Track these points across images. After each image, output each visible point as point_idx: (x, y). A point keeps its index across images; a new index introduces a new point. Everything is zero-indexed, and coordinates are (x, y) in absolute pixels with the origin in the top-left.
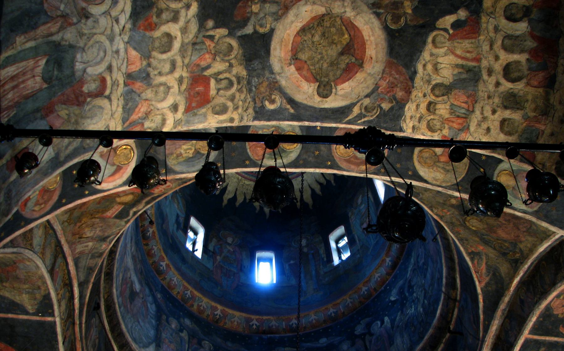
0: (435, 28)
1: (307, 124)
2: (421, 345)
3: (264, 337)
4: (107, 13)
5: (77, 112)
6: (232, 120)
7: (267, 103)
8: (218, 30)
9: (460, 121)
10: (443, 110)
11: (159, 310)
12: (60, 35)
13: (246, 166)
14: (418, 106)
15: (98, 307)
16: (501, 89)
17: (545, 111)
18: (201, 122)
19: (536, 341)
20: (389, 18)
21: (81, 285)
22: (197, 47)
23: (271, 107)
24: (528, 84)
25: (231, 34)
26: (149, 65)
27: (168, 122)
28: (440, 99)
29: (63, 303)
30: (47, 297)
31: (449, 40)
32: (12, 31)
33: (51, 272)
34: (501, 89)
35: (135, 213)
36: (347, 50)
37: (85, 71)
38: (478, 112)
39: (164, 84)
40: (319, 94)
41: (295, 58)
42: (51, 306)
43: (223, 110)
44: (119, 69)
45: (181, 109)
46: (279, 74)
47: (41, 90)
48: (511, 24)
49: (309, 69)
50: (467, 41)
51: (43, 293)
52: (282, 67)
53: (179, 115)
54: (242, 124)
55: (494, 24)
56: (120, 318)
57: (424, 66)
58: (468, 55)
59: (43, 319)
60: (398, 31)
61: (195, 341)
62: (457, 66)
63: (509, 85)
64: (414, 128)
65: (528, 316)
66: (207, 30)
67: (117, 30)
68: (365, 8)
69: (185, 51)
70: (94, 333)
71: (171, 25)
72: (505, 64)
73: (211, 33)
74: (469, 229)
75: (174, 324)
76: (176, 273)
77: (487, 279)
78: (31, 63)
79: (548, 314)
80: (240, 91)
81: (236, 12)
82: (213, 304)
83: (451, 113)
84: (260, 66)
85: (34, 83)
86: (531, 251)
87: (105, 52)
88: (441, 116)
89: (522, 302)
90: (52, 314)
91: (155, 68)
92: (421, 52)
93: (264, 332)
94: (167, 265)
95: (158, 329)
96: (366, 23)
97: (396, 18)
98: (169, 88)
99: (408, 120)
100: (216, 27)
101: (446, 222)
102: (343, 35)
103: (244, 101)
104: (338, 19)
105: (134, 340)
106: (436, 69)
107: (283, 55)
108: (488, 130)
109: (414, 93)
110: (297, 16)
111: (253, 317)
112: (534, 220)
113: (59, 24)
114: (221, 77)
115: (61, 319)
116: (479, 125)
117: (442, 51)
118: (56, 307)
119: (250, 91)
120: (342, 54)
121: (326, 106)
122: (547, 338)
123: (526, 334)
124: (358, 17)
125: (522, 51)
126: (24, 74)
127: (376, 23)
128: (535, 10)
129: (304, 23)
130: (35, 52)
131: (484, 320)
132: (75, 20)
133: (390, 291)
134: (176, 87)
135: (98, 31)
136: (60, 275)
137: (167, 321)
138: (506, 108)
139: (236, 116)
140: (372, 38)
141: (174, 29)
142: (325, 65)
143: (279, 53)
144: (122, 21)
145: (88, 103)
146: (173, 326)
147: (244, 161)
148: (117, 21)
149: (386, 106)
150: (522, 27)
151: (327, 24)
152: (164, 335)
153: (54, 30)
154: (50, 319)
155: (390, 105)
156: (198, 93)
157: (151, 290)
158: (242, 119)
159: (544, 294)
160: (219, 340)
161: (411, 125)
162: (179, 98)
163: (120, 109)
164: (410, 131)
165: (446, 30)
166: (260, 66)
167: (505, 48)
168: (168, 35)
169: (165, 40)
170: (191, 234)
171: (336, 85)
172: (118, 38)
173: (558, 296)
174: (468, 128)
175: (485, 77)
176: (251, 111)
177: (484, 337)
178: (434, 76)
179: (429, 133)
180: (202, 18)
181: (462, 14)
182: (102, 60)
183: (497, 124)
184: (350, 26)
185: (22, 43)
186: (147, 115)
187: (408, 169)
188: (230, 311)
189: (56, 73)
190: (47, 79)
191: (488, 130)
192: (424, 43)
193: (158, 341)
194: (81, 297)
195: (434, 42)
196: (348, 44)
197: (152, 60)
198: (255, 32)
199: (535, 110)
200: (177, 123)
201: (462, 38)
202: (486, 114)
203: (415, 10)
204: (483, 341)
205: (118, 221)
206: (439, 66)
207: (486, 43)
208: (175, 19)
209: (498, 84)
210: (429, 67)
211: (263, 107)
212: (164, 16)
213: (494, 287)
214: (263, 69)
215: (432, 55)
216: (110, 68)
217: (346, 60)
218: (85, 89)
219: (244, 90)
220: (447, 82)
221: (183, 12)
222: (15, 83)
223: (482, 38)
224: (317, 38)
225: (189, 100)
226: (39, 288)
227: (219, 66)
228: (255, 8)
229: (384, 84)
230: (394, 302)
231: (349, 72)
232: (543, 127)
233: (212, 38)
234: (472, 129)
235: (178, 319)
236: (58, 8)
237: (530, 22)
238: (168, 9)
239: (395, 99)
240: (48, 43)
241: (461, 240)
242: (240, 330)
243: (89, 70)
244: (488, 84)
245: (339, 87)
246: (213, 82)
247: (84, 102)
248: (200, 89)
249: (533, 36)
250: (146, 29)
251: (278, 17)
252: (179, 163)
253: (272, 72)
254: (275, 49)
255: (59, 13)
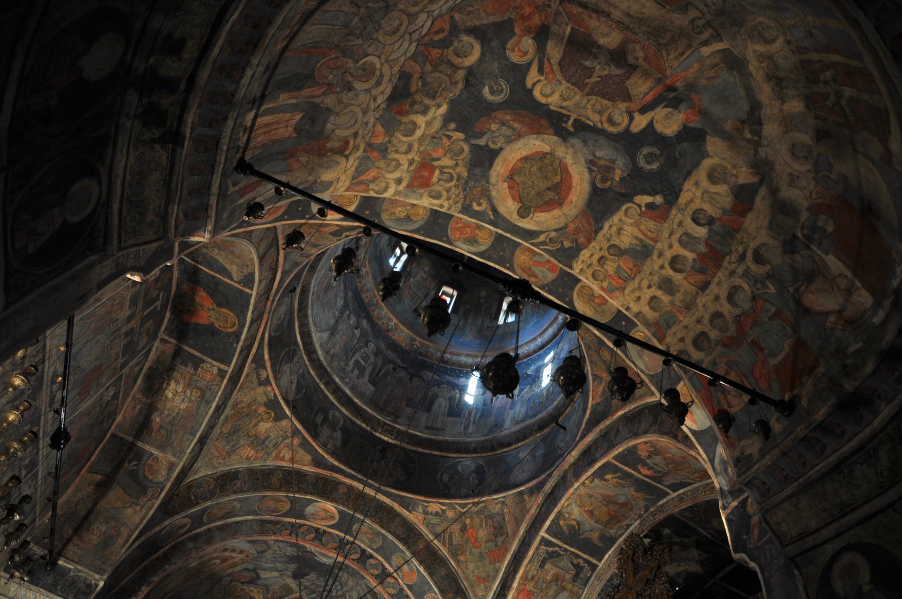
0: (632, 201)
1: (500, 231)
2: (533, 420)
3: (420, 357)
4: (368, 91)
5: (315, 161)
6: (442, 206)
7: (474, 204)
8: (457, 133)
9: (620, 281)
10: (610, 267)
11: (346, 305)
12: (322, 98)
13: (442, 241)
14: (592, 255)
15: (294, 290)
16: (663, 272)
17: (689, 306)
18: (416, 199)
19: (616, 466)
20: (599, 177)
21: (284, 273)
22: (435, 141)
23: (476, 208)
24: (686, 278)
25: (466, 140)
26: (390, 142)
27: (390, 190)
28: (612, 257)
29: (263, 284)
30: (252, 275)
31: (639, 215)
32: (279, 88)
33: (261, 259)
34: (663, 272)
35: (347, 236)
36: (556, 188)
37: (333, 131)
38: (637, 281)
39: (397, 161)
40: (518, 213)
41: (510, 178)
42: (253, 283)
43: (438, 196)
44: (363, 137)
45: (404, 184)
46: (493, 185)
47: (290, 138)
48: (694, 225)
49: (518, 191)
50: (653, 222)
51: (249, 270)
52: (498, 181)
53: (401, 188)
54: (449, 212)
55: (680, 217)
56: (310, 303)
57: (611, 226)
58: (649, 234)
59: (243, 288)
60: (602, 190)
61: (364, 340)
62: (637, 238)
63: (671, 272)
64: (581, 270)
65: (617, 445)
66: (448, 130)
67: (372, 106)
68: (582, 161)
69: (424, 140)
70: (283, 309)
71: (419, 116)
72: (675, 254)
73: (450, 133)
74: (600, 357)
75: (353, 321)
76: (371, 280)
77: (599, 400)
78: (288, 115)
79: (633, 450)
80: (457, 186)
81: (477, 124)
82: (391, 316)
83: (615, 272)
84: (480, 174)
85: (285, 132)
86: (641, 397)
87: (356, 121)
88: (607, 270)
89: (618, 431)
90: (252, 290)
91: (394, 146)
92: (613, 214)
93: (421, 354)
94: (367, 273)
95: (337, 321)
96: (579, 174)
97: (604, 180)
98: (400, 164)
99: (579, 263)
100: (456, 130)
101: (585, 344)
102: (557, 175)
103: (457, 196)
104: (557, 161)
105: (315, 324)
106: (619, 231)
107: (502, 171)
108: (639, 298)
109: (593, 244)
110: (525, 145)
111: (417, 338)
112: (647, 381)
113: (323, 90)
114: (445, 170)
115: (257, 293)
116: (633, 291)
117: (630, 221)
118: (256, 284)
119: (465, 190)
120: (549, 189)
121: (520, 224)
122: (626, 468)
123: (609, 458)
124: (574, 166)
125: (692, 251)
126: (279, 123)
127: (587, 176)
128: (718, 223)
129: (529, 153)
130: (294, 108)
131: (584, 429)
132: (338, 90)
133: (530, 365)
134: (406, 166)
135: (355, 103)
136: (269, 260)
137: (348, 317)
138: (660, 288)
139: (446, 204)
140: (578, 187)
141: (421, 120)
142: (533, 193)
143: (499, 169)
144: (379, 101)
145: (328, 157)
146: (351, 322)
147: (443, 237)
148: (375, 99)
149: (567, 244)
150: (701, 232)
151: (547, 161)
152: (341, 327)
153: (317, 93)
154: (248, 291)
155: (570, 245)
156: (422, 177)
157: (345, 287)
158: (449, 208)
159: (636, 435)
160: (383, 346)
161: (580, 267)
162: (405, 174)
163: (353, 169)
164: (577, 271)
165: (640, 206)
166: (480, 174)
167: (680, 241)
168: (414, 123)
169: (410, 126)
170: (398, 251)
171: (535, 211)
172: (370, 113)
173: (646, 443)
174: (624, 290)
175: (655, 257)
176: (459, 205)
177: (579, 442)
178: (614, 238)
179: (592, 280)
180: (447, 119)
181: (659, 199)
182: (352, 126)
183: (648, 297)
184: (564, 170)
185: (285, 99)
186: (374, 179)
187: (567, 296)
188: (402, 327)
189: (307, 127)
190: (298, 129)
191: (639, 298)
192: (618, 208)
193: (333, 331)
194: (282, 281)
195: (626, 211)
196: (557, 184)
197: (394, 139)
198: (487, 145)
199: (682, 301)
200: (397, 193)
201: (650, 218)
202: (642, 286)
203: (622, 179)
204: (577, 444)
205: (331, 237)
206: (622, 232)
207: (667, 231)
208: (424, 112)
209: (662, 267)
210: (614, 229)
211: (471, 205)
212: (416, 107)
213: (602, 408)
214: (482, 176)
215: (620, 220)
216: (356, 135)
217: (551, 195)
218: (329, 145)
219: (460, 187)
220: (623, 247)
221: (433, 110)
222: (268, 129)
223: (666, 225)
224: (534, 169)
225: (413, 179)
226: (248, 266)
227: (447, 161)
228: (494, 127)
229: (572, 227)
230: (529, 376)
231: (548, 206)
232: (682, 318)
233: (449, 137)
234: (626, 292)
235: (358, 317)
236: (326, 78)
237: (710, 230)
238: (421, 103)
239: (576, 242)
240: (308, 103)
241: (591, 362)
242: (403, 344)
243: (337, 132)
244: (654, 263)
245: (536, 214)
246: (437, 172)
247: (324, 155)
248: (426, 174)
249: (707, 244)
250: (397, 113)
251: (510, 141)
252: (390, 220)
253: (488, 182)
254: (497, 165)
255: (326, 81)
